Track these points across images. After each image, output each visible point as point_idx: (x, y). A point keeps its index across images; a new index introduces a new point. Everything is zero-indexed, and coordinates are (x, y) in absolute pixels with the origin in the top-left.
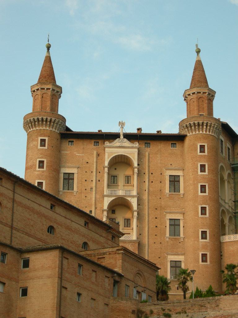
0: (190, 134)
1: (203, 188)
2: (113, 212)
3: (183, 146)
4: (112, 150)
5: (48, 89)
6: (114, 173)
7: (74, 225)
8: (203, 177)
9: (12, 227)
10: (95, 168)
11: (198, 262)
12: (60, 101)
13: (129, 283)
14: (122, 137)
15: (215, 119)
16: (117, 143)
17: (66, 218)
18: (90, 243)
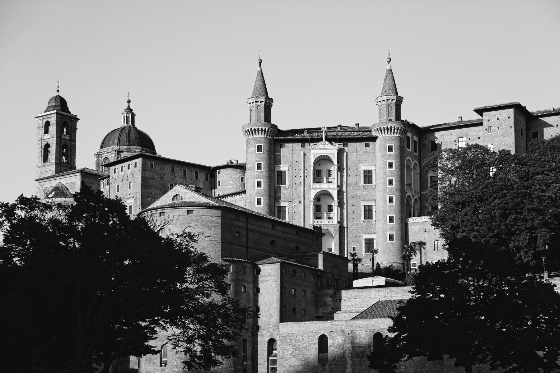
0: (381, 136)
1: (391, 182)
3: (375, 145)
4: (315, 151)
5: (261, 102)
6: (319, 168)
7: (289, 236)
8: (391, 172)
9: (247, 247)
10: (303, 166)
11: (387, 240)
12: (271, 108)
13: (329, 275)
14: (324, 140)
15: (403, 121)
16: (320, 145)
17: (282, 232)
18: (300, 246)
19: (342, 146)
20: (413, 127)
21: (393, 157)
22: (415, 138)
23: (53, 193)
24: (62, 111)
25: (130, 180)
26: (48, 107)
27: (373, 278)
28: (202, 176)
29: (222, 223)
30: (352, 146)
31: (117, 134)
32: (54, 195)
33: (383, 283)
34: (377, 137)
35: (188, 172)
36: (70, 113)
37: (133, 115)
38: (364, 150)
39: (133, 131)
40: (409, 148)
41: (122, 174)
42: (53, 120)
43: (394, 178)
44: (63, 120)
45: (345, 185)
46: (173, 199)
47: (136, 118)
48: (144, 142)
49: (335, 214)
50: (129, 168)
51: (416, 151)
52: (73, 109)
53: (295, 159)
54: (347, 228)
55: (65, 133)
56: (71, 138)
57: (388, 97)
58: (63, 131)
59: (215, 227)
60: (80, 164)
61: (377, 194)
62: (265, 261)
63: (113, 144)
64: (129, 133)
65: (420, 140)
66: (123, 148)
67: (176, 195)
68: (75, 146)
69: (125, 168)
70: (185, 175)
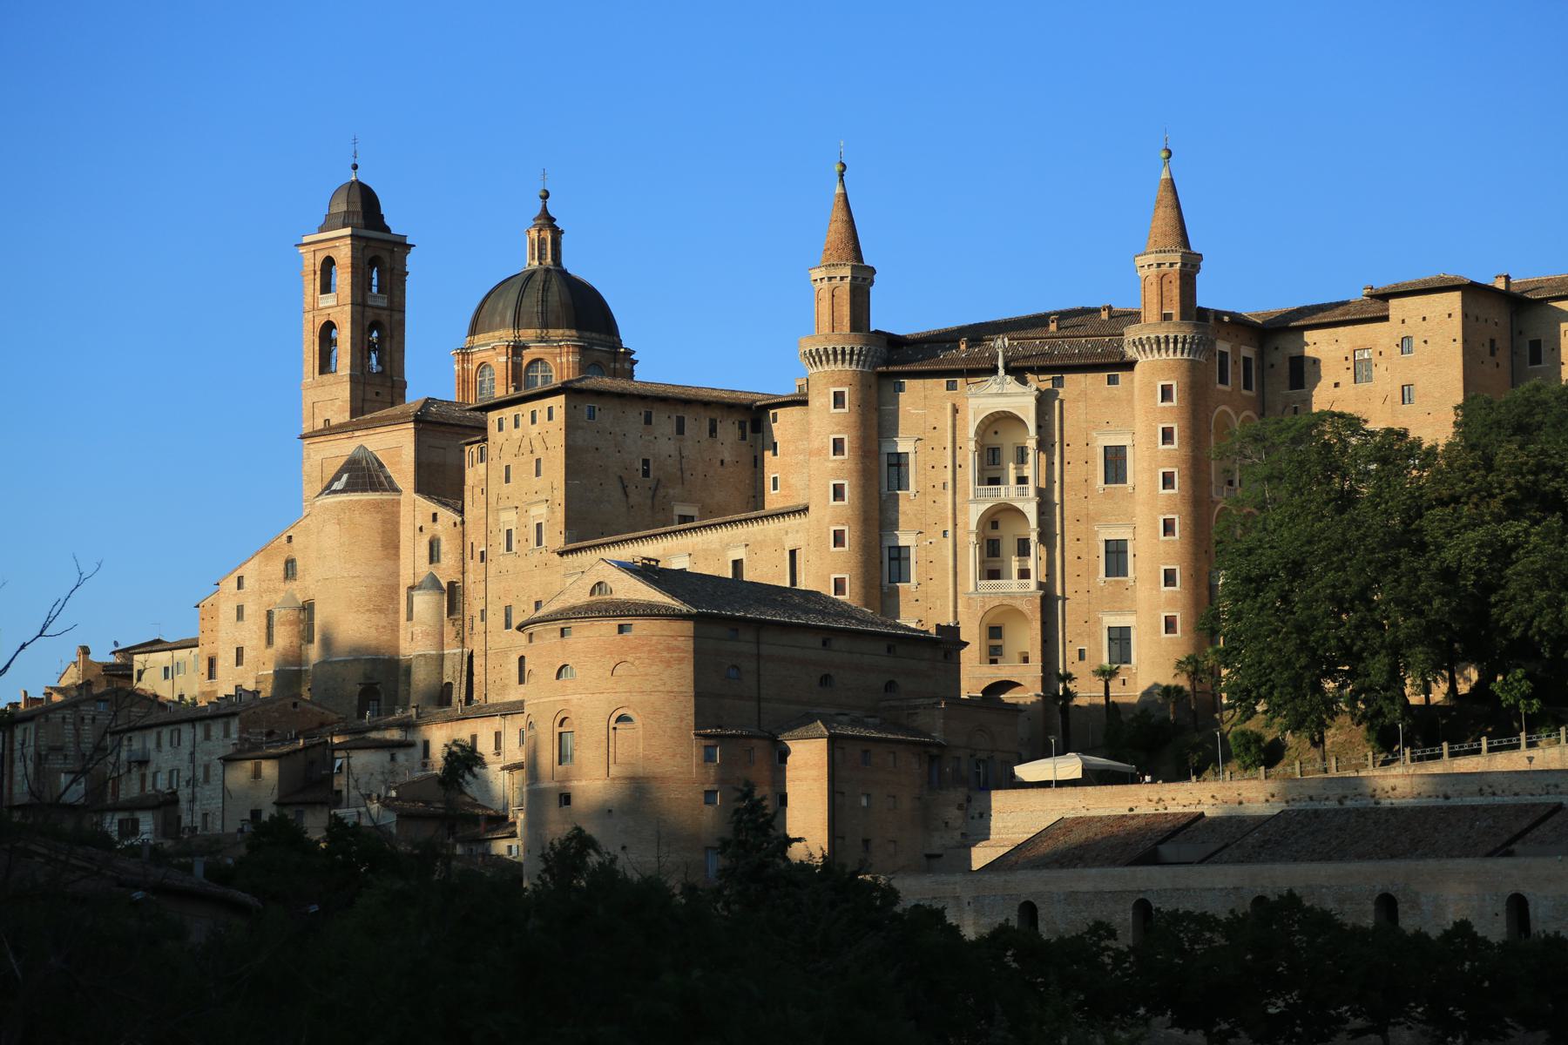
2: (995, 525)
3: (1132, 381)
5: (842, 278)
6: (993, 441)
9: (759, 700)
14: (1001, 372)
16: (992, 384)
19: (1049, 385)
20: (1238, 324)
21: (1171, 414)
22: (1247, 351)
23: (345, 477)
24: (366, 227)
25: (539, 453)
26: (329, 216)
27: (1059, 759)
28: (729, 431)
29: (696, 651)
30: (1074, 384)
31: (513, 295)
32: (347, 483)
33: (1077, 774)
34: (1135, 362)
35: (689, 424)
36: (387, 229)
37: (557, 234)
38: (1105, 393)
39: (555, 286)
40: (1223, 380)
41: (517, 433)
42: (343, 254)
43: (1176, 471)
44: (370, 254)
45: (1057, 486)
46: (592, 593)
47: (564, 239)
48: (585, 313)
49: (1035, 561)
50: (533, 422)
51: (1247, 386)
52: (396, 220)
53: (932, 422)
54: (1064, 599)
55: (375, 289)
56: (391, 301)
57: (1161, 257)
58: (371, 285)
59: (681, 660)
60: (415, 395)
61: (1138, 509)
62: (796, 732)
63: (502, 325)
64: (545, 290)
65: (1261, 355)
66: (528, 334)
67: (599, 584)
68: (402, 323)
69: (525, 420)
70: (680, 430)
